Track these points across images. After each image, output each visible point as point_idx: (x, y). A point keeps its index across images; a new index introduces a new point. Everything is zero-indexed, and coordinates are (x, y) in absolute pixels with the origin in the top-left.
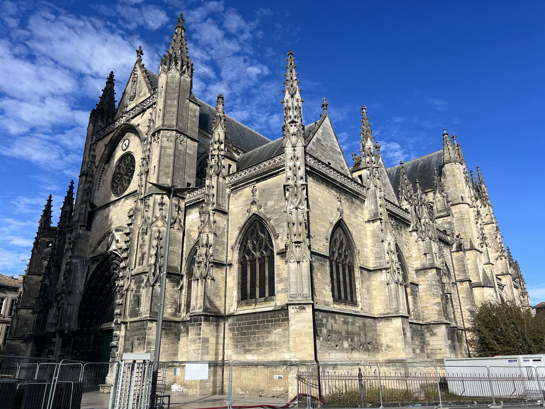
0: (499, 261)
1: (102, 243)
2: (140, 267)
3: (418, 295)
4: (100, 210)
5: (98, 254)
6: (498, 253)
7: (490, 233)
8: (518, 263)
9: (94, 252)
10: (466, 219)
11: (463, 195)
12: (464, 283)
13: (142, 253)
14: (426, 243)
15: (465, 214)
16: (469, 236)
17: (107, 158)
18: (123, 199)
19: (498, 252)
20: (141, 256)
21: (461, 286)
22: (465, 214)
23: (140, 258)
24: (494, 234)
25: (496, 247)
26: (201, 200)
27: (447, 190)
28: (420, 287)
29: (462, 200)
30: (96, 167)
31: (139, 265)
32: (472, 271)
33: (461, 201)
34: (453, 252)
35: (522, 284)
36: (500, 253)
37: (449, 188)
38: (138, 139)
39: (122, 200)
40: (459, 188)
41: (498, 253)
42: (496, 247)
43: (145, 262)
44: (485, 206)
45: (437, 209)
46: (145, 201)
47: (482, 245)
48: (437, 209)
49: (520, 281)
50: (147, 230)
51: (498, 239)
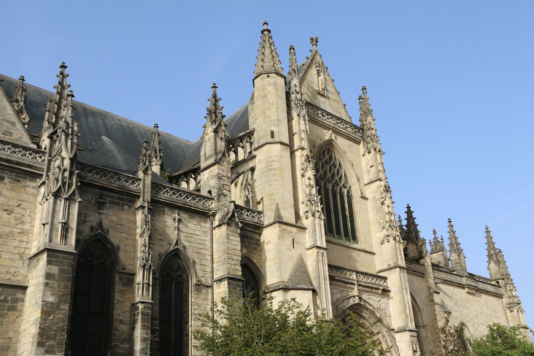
0: (386, 244)
3: (19, 307)
6: (385, 232)
7: (375, 197)
8: (503, 253)
10: (275, 169)
11: (274, 129)
12: (222, 283)
14: (49, 204)
15: (274, 161)
16: (275, 199)
19: (385, 231)
21: (218, 290)
22: (274, 161)
24: (379, 199)
25: (382, 221)
27: (254, 124)
28: (28, 291)
29: (273, 136)
32: (272, 263)
33: (270, 140)
34: (214, 228)
35: (508, 288)
36: (387, 230)
37: (256, 119)
40: (269, 117)
41: (385, 232)
42: (382, 221)
44: (369, 152)
45: (205, 154)
47: (307, 214)
48: (205, 154)
49: (506, 284)
51: (385, 207)
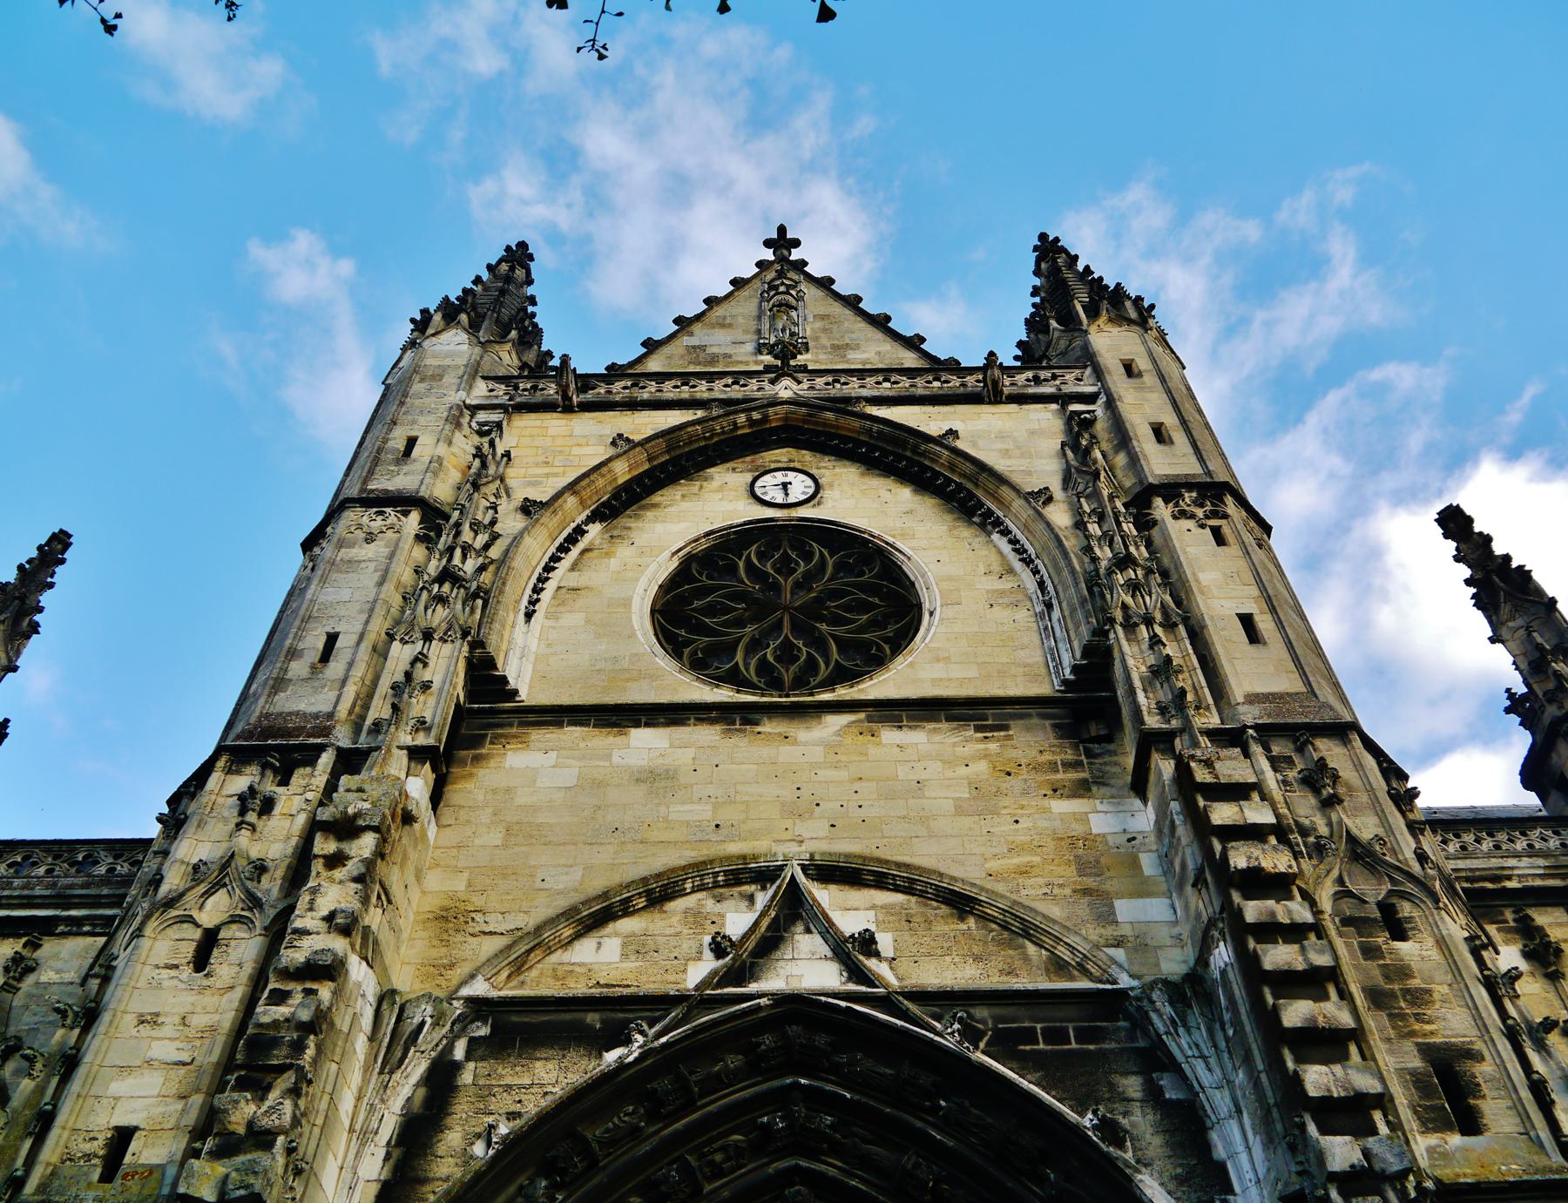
1: (626, 925)
2: (1455, 1140)
4: (560, 724)
5: (579, 988)
9: (519, 966)
13: (1426, 1051)
17: (616, 495)
18: (862, 716)
20: (1416, 1063)
23: (1417, 1081)
26: (1512, 884)
30: (528, 508)
31: (1433, 1122)
38: (905, 494)
39: (835, 722)
43: (1494, 1109)
46: (1267, 749)
50: (1387, 908)
